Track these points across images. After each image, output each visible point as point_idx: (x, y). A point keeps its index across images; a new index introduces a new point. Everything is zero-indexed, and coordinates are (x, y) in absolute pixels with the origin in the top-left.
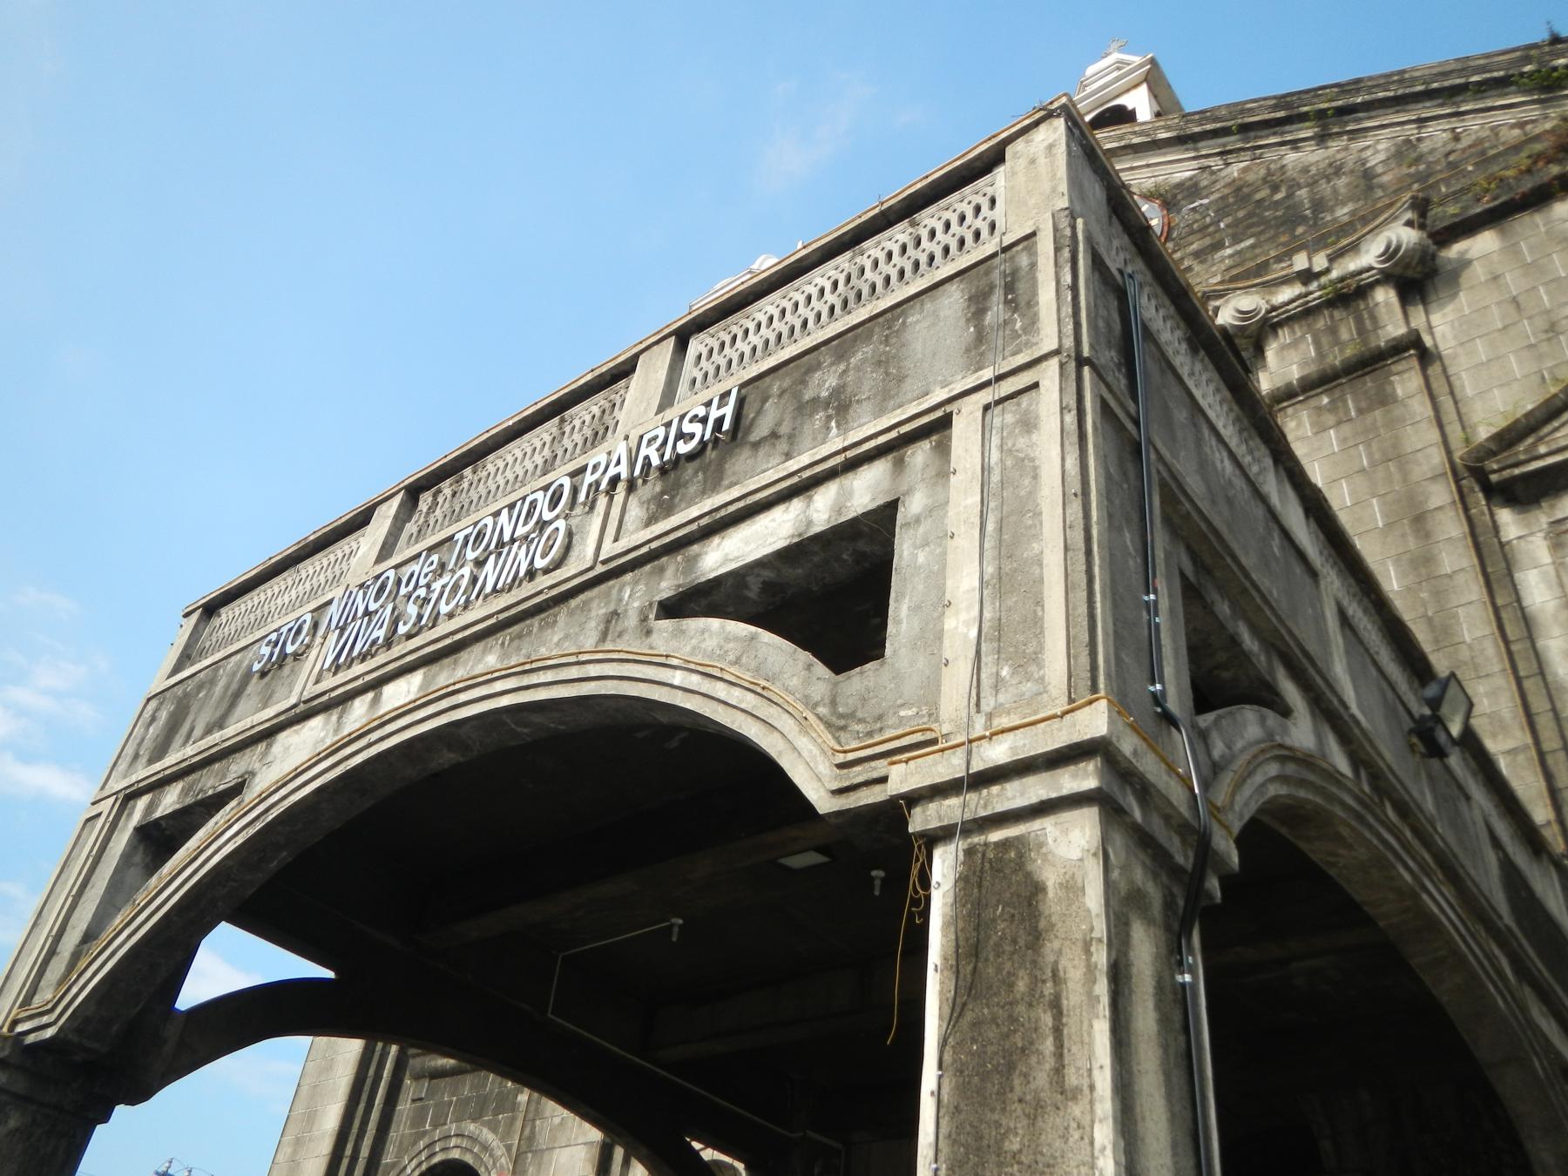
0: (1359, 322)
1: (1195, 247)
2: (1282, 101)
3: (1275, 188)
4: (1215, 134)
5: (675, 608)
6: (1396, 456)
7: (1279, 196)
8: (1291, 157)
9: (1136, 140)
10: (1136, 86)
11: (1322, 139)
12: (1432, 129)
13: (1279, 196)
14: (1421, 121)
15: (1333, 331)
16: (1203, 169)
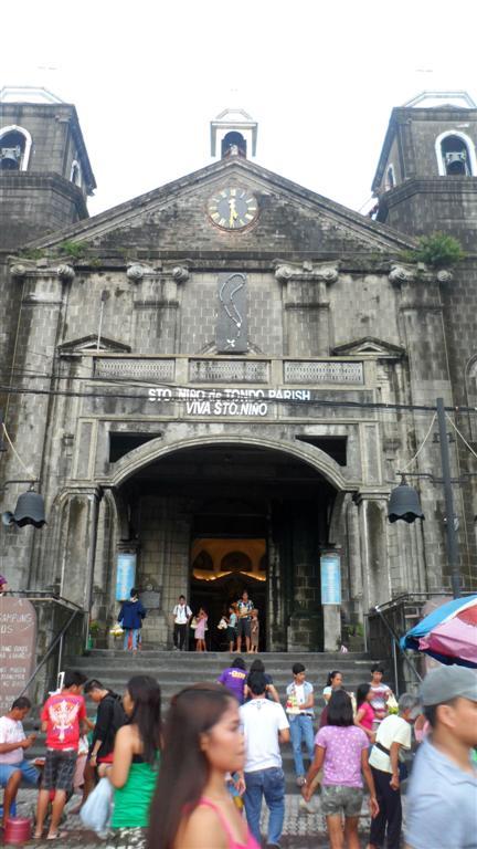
0: (315, 291)
1: (266, 227)
2: (305, 190)
3: (295, 220)
4: (280, 186)
5: (298, 437)
6: (316, 339)
7: (295, 224)
8: (301, 210)
9: (255, 171)
10: (248, 128)
11: (313, 209)
12: (341, 227)
13: (295, 224)
14: (340, 223)
15: (307, 290)
16: (273, 195)
